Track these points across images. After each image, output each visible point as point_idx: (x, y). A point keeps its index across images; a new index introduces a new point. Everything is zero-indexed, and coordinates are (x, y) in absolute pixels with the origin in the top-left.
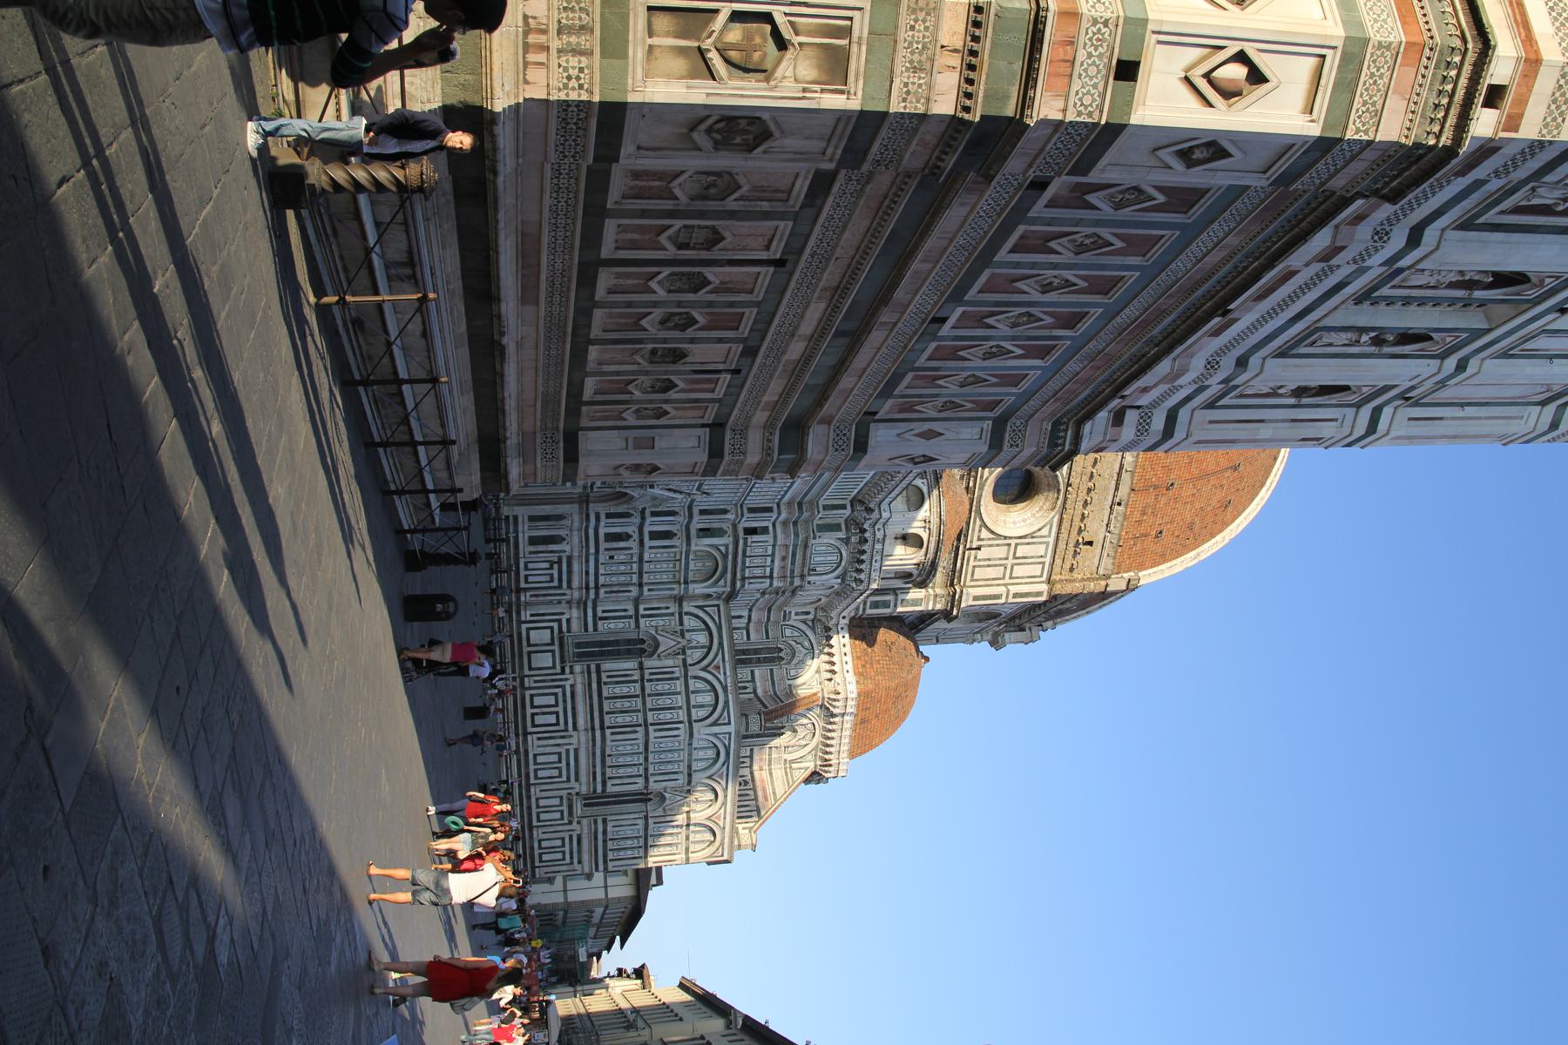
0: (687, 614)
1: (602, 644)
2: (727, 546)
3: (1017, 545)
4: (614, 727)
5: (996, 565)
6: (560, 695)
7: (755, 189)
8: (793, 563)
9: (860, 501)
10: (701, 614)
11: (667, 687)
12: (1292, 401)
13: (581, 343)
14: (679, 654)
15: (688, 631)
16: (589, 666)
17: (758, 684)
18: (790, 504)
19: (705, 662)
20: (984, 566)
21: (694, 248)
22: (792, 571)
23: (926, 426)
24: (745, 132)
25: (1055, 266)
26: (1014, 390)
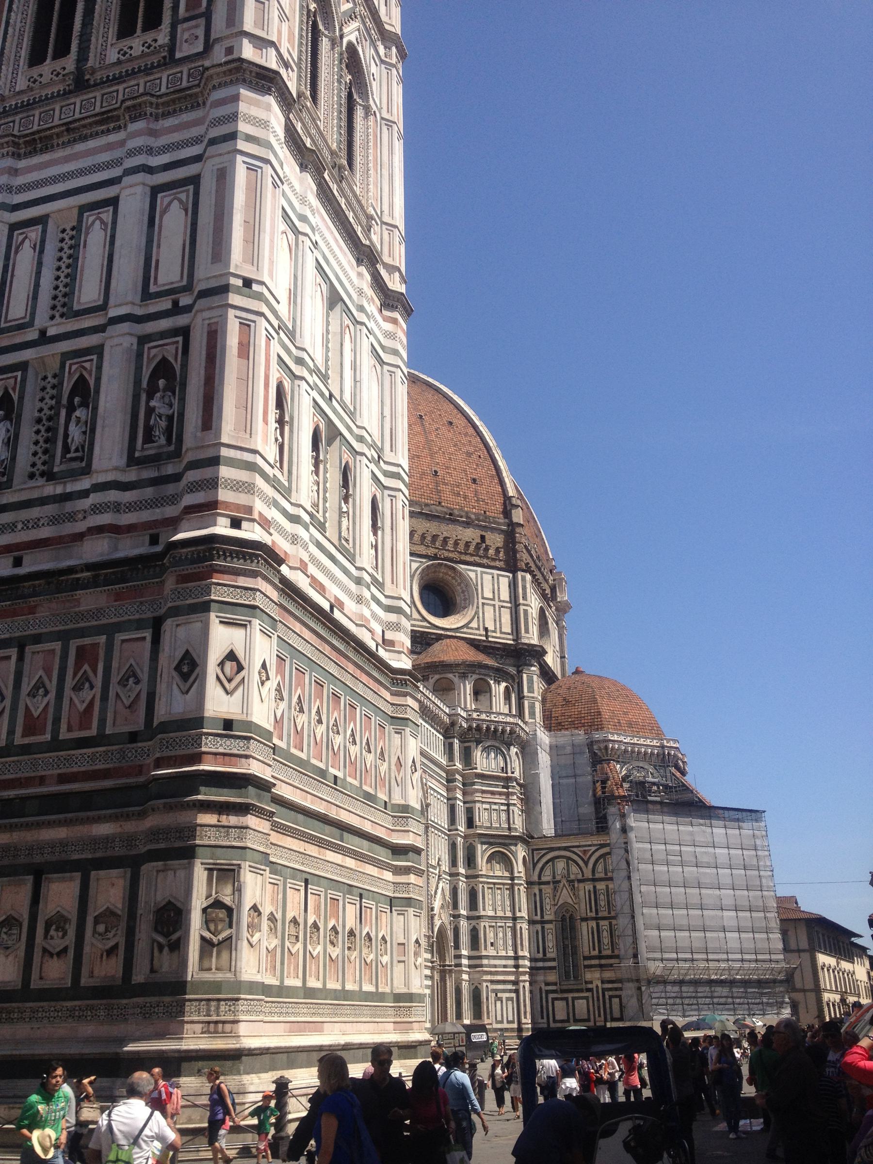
3: (483, 598)
5: (500, 614)
7: (272, 904)
8: (497, 786)
9: (446, 731)
10: (540, 865)
12: (380, 533)
13: (344, 994)
14: (573, 886)
15: (554, 877)
16: (586, 967)
18: (448, 790)
20: (500, 624)
21: (298, 933)
22: (503, 787)
23: (393, 767)
24: (253, 918)
25: (310, 723)
26: (373, 719)
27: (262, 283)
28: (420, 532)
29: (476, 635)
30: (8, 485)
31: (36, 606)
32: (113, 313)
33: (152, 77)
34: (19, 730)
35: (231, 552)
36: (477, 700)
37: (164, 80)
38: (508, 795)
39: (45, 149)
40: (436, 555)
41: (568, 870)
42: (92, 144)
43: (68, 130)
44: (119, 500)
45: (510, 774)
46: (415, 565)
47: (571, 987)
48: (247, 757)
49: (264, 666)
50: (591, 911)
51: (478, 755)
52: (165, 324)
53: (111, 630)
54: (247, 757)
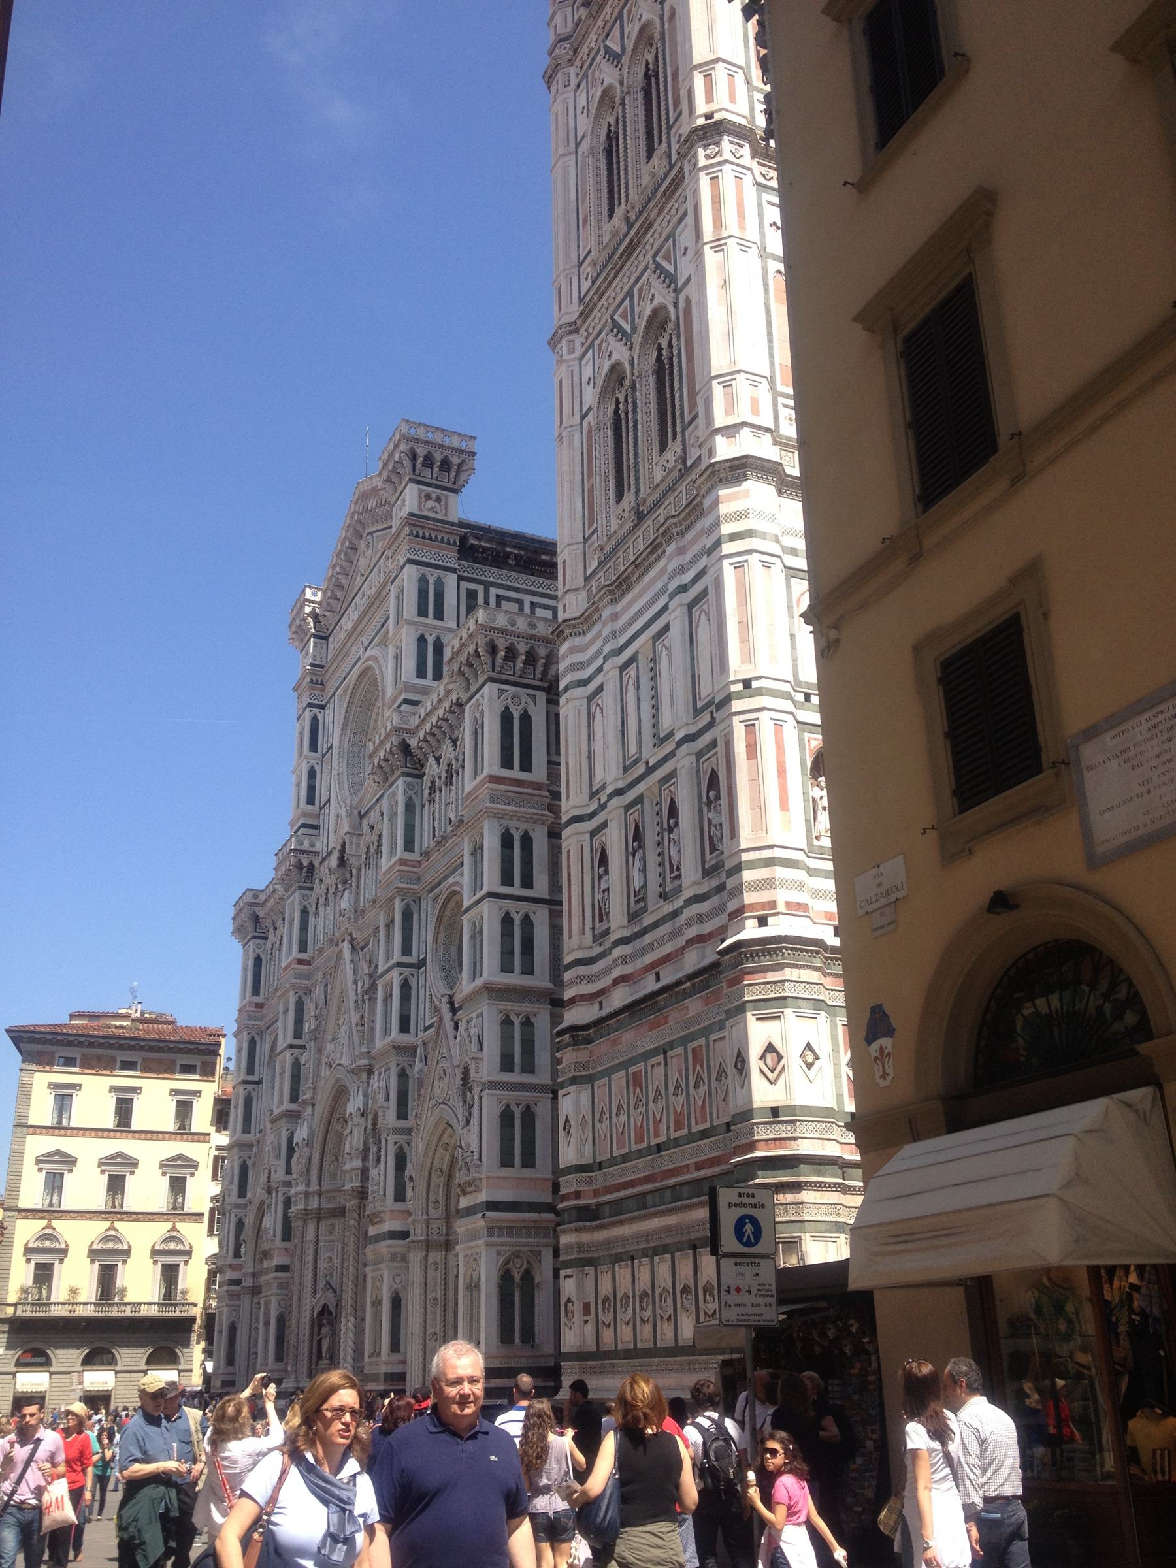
27: (760, 677)
30: (644, 910)
31: (667, 1017)
32: (678, 736)
33: (677, 493)
34: (672, 1129)
35: (757, 952)
37: (684, 492)
39: (629, 588)
42: (652, 573)
43: (636, 567)
44: (700, 911)
48: (795, 1139)
49: (809, 1046)
52: (707, 738)
53: (706, 1032)
54: (795, 1139)
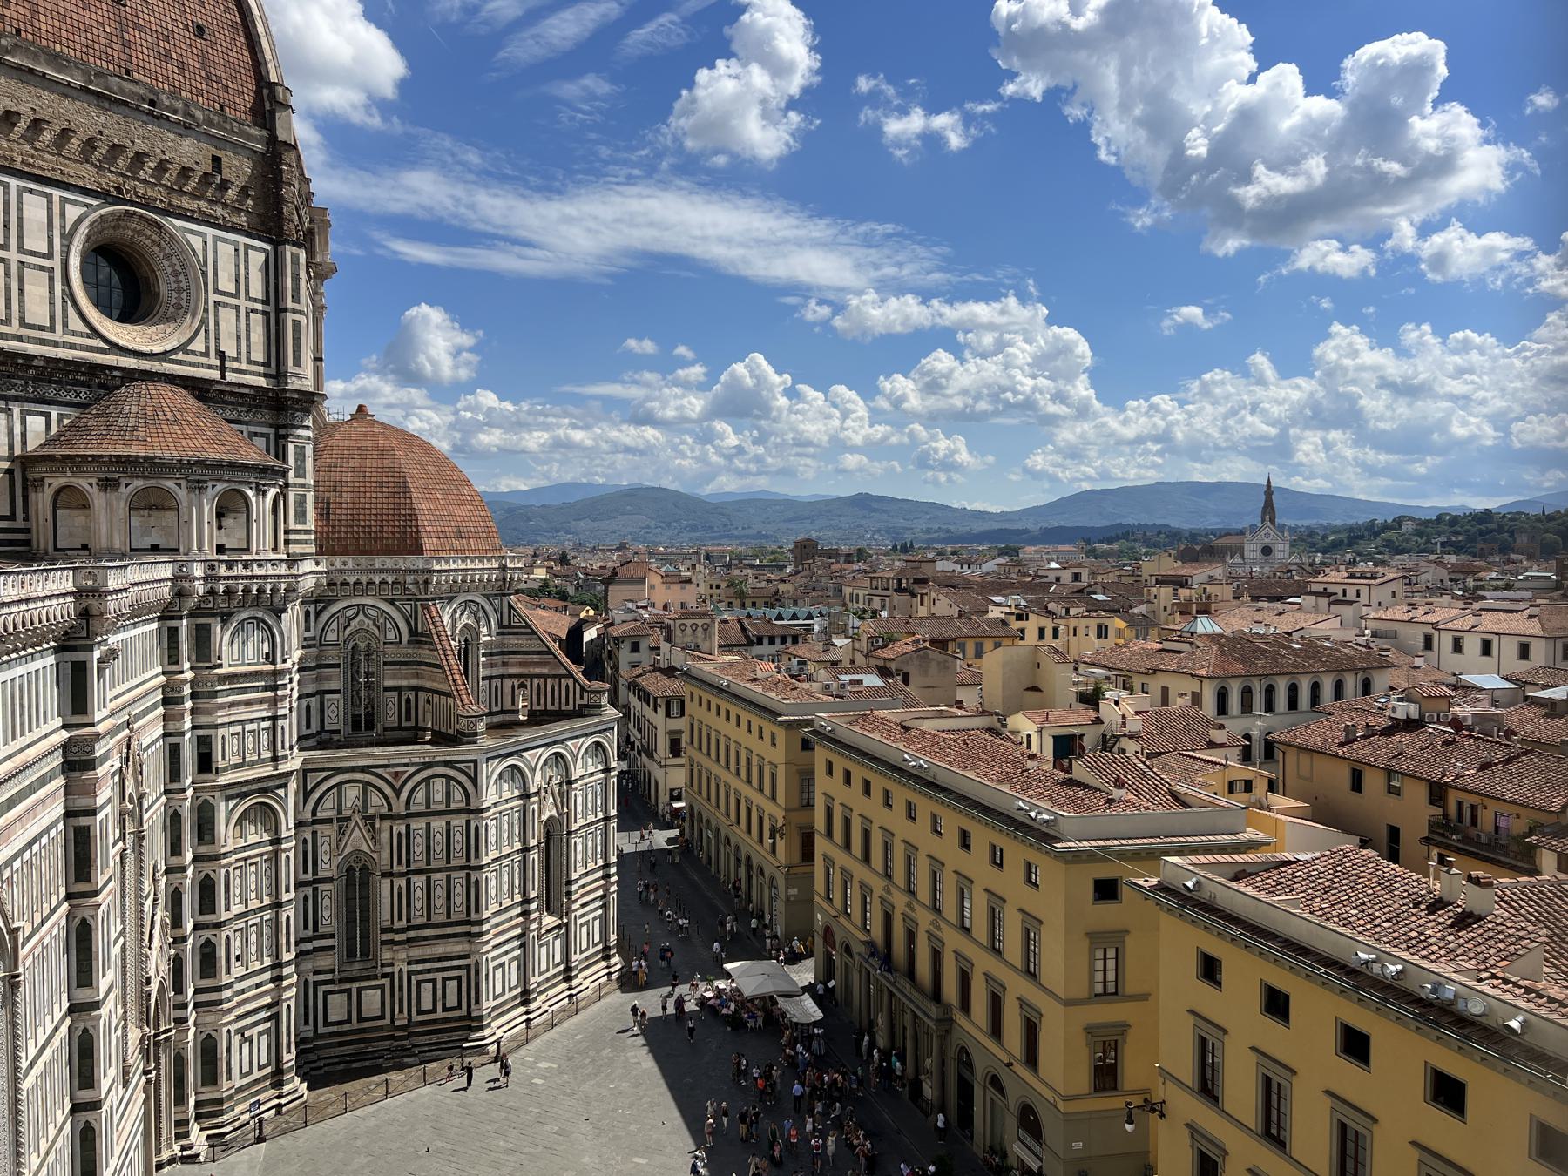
0: (314, 813)
1: (350, 921)
2: (228, 799)
3: (217, 291)
4: (468, 908)
5: (248, 325)
6: (420, 977)
10: (316, 795)
11: (418, 840)
14: (373, 825)
15: (340, 812)
16: (384, 943)
17: (404, 683)
19: (388, 791)
20: (248, 346)
22: (266, 688)
28: (83, 134)
29: (202, 366)
36: (220, 527)
38: (274, 702)
40: (118, 189)
41: (365, 801)
45: (280, 666)
46: (73, 213)
47: (355, 974)
50: (400, 862)
51: (221, 636)
